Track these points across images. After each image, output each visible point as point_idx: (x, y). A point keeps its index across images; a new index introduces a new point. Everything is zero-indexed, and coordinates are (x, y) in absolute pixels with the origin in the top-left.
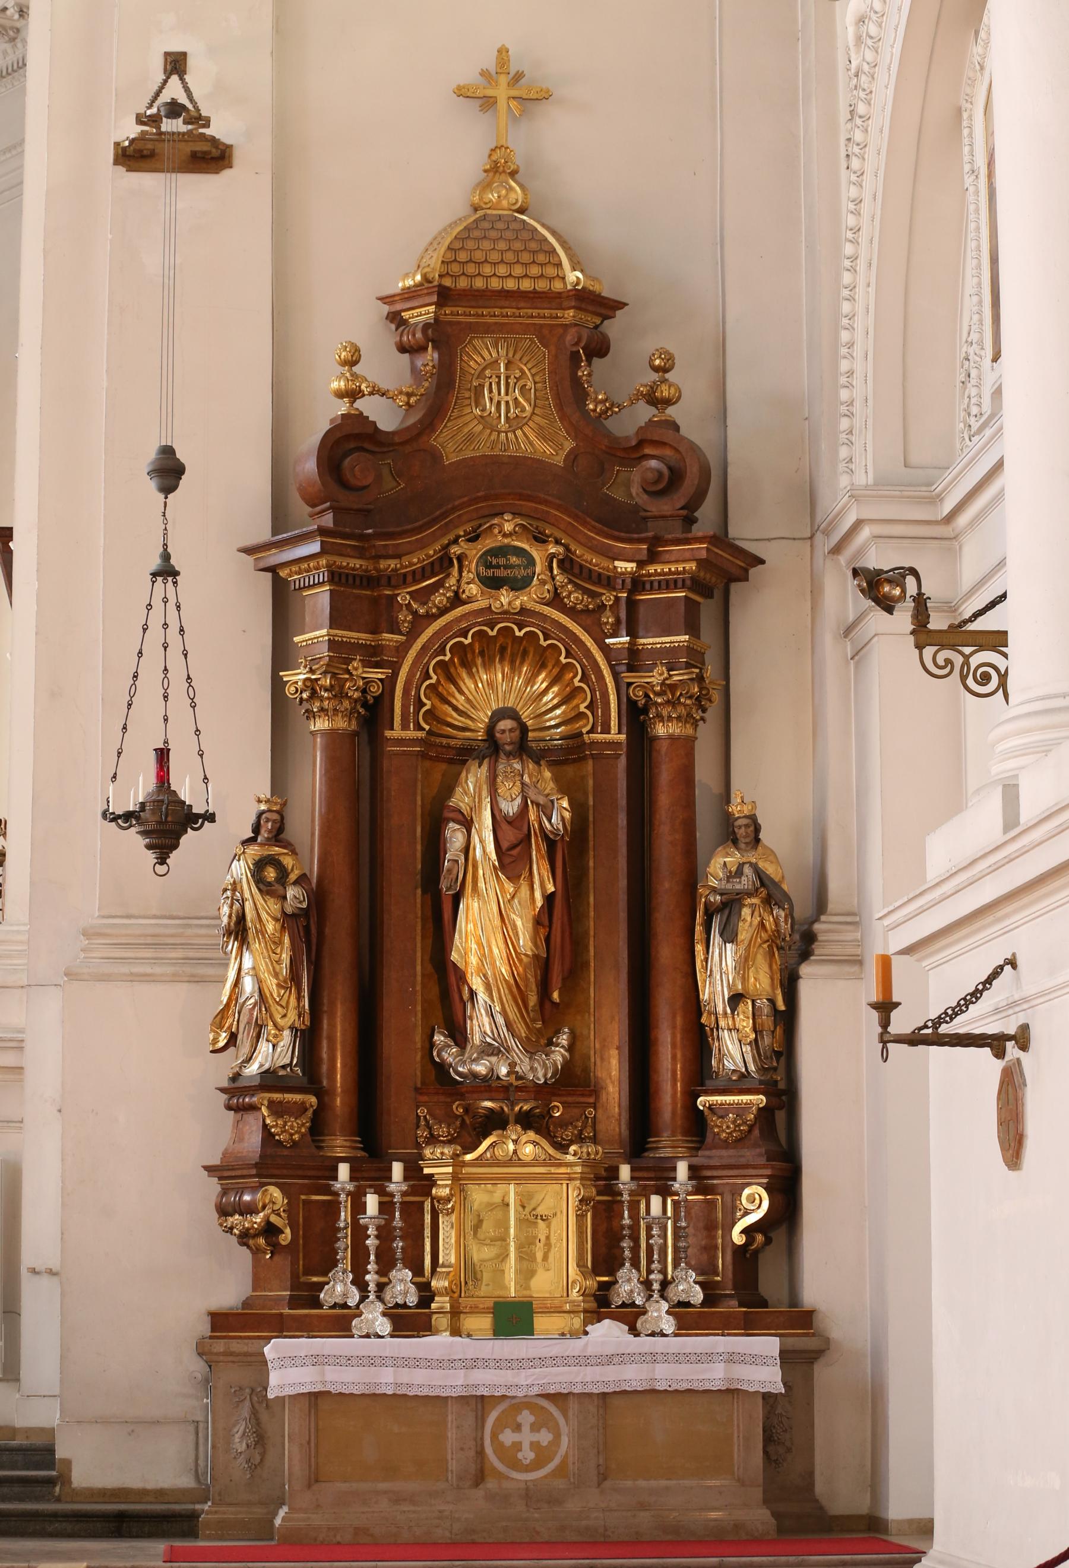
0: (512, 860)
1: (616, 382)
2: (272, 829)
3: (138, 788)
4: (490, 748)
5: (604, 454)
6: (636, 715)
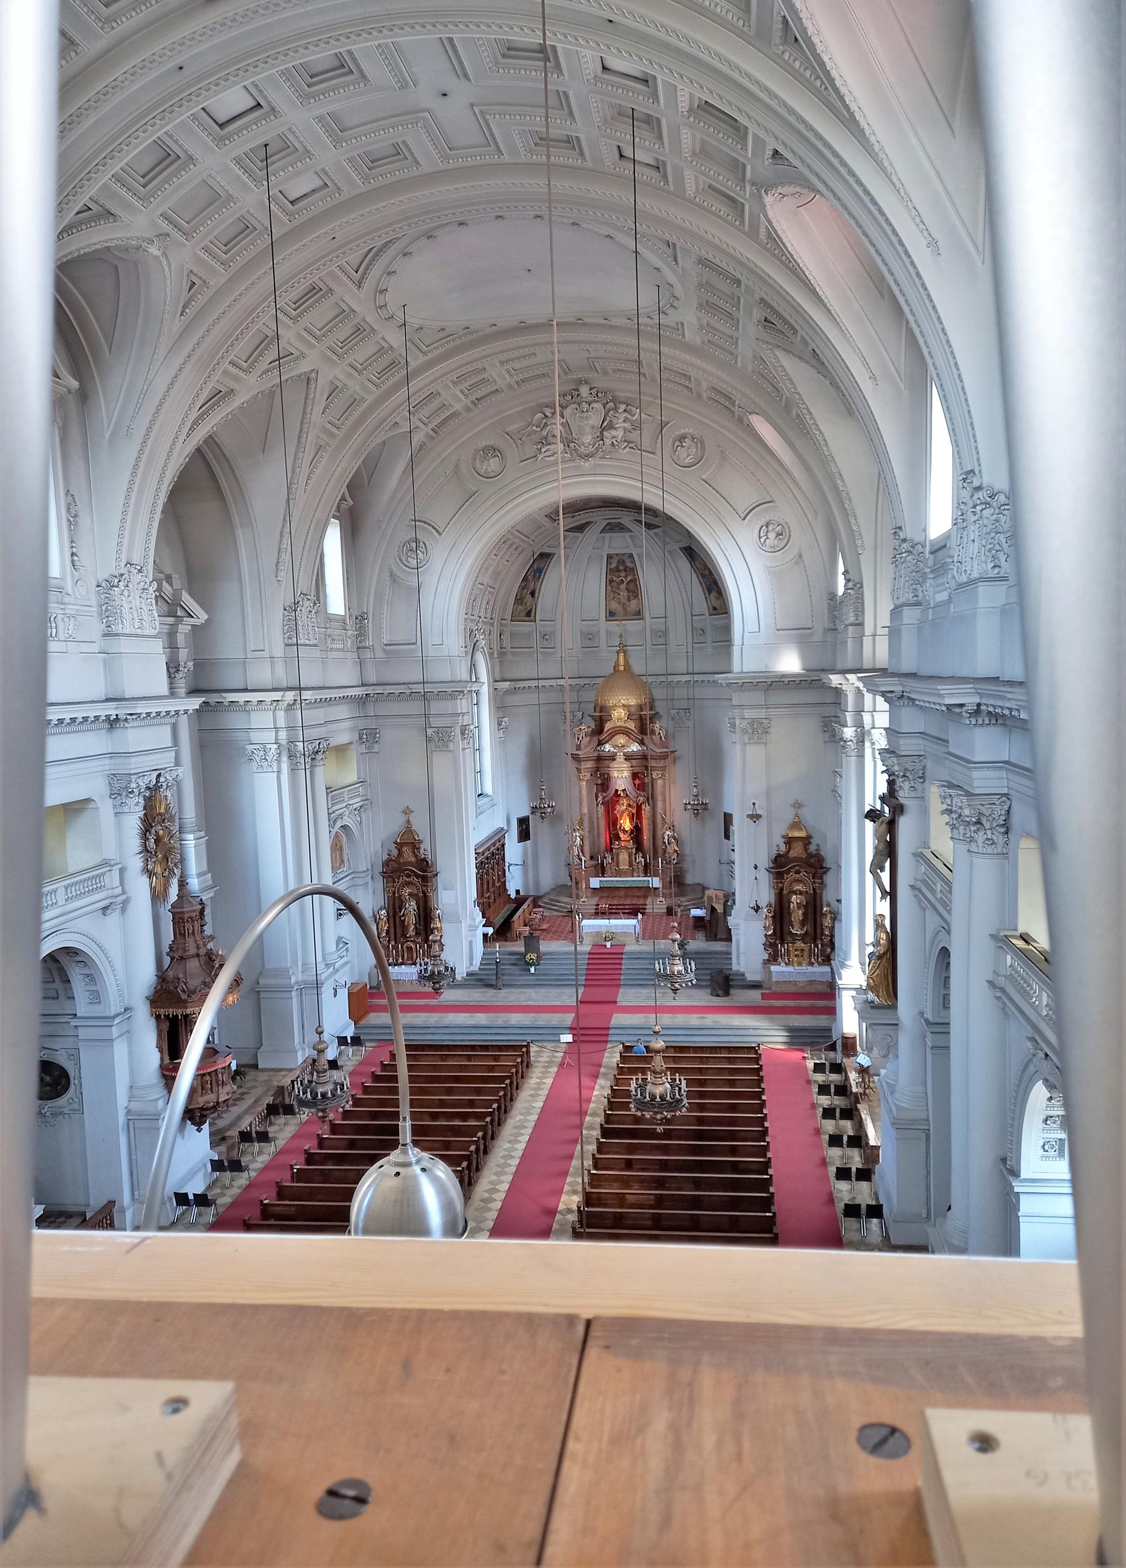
0: (799, 908)
1: (812, 848)
2: (769, 905)
3: (753, 904)
4: (795, 893)
5: (811, 856)
6: (814, 889)
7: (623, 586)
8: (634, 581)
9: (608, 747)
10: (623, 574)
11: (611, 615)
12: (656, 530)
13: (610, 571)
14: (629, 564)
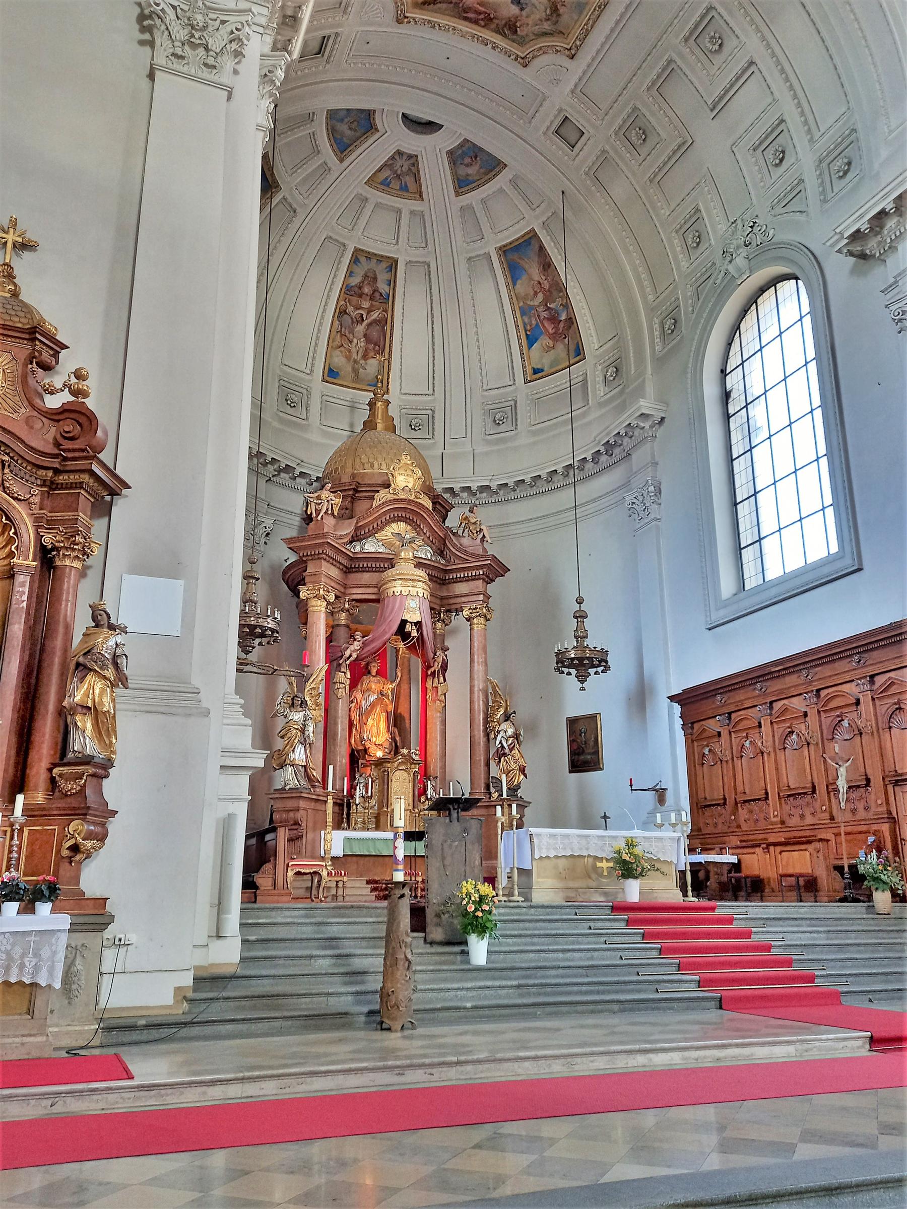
7: (360, 329)
8: (383, 324)
9: (370, 547)
10: (366, 304)
11: (331, 374)
12: (473, 198)
13: (349, 291)
14: (383, 287)
